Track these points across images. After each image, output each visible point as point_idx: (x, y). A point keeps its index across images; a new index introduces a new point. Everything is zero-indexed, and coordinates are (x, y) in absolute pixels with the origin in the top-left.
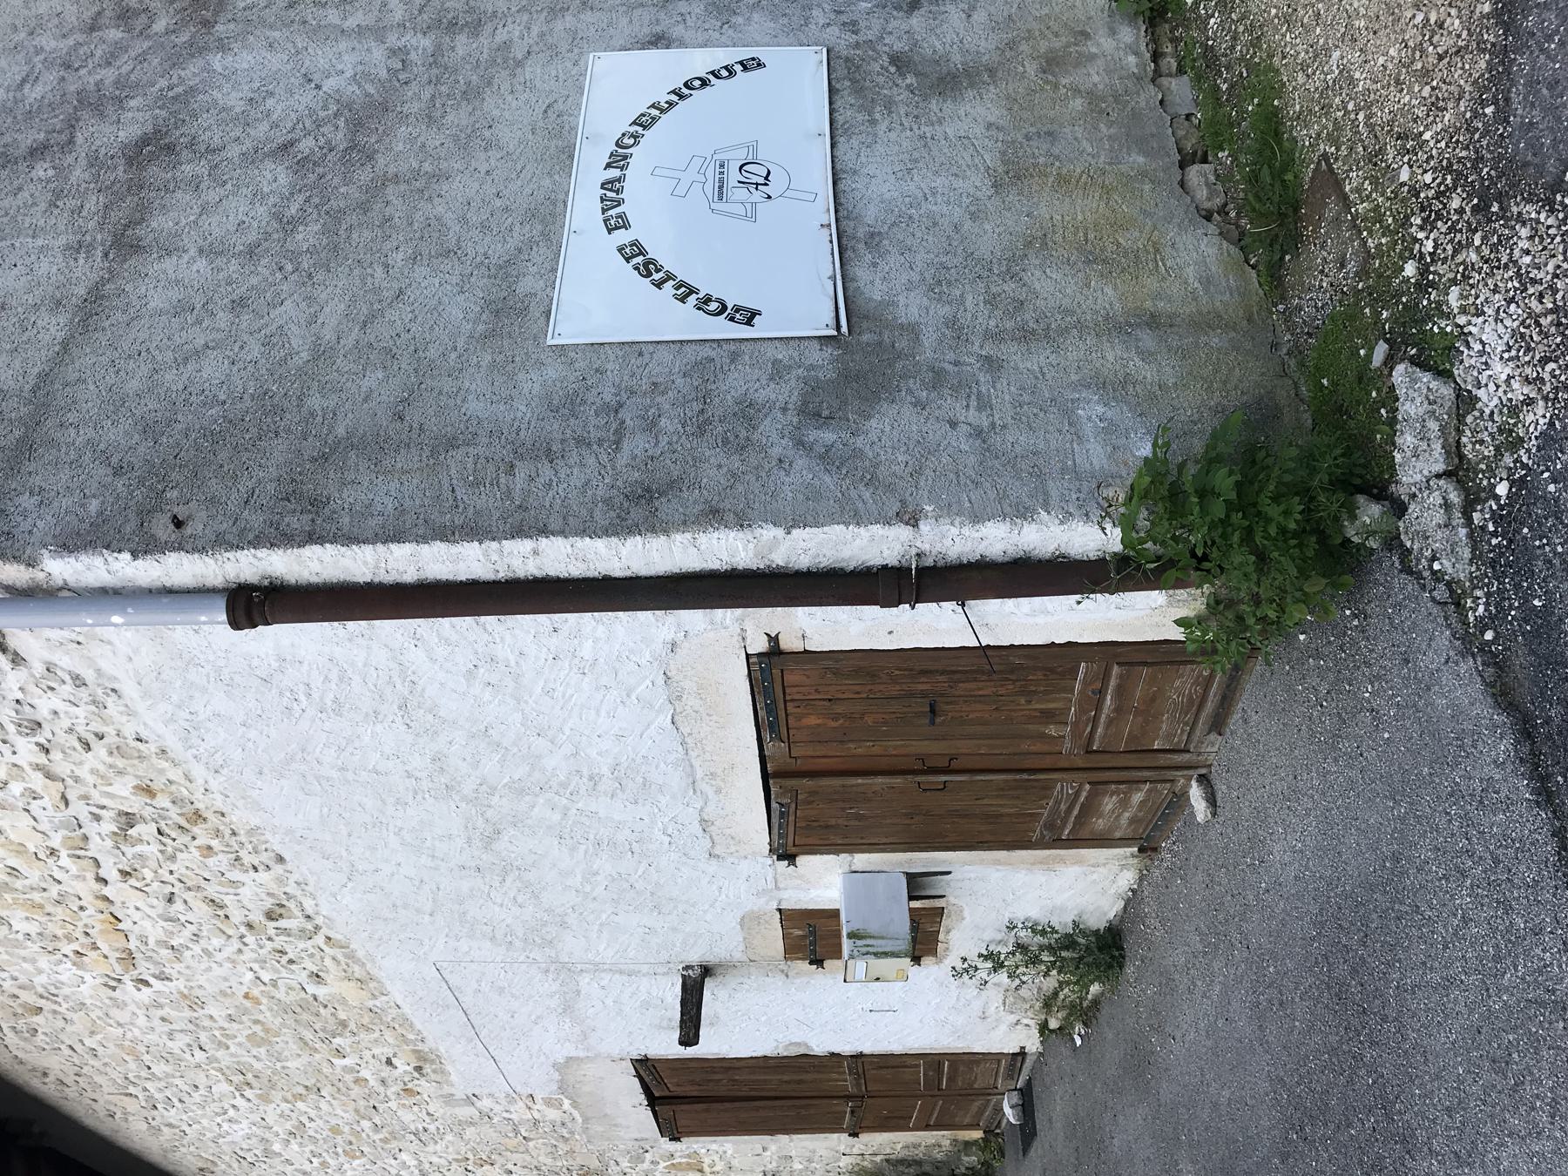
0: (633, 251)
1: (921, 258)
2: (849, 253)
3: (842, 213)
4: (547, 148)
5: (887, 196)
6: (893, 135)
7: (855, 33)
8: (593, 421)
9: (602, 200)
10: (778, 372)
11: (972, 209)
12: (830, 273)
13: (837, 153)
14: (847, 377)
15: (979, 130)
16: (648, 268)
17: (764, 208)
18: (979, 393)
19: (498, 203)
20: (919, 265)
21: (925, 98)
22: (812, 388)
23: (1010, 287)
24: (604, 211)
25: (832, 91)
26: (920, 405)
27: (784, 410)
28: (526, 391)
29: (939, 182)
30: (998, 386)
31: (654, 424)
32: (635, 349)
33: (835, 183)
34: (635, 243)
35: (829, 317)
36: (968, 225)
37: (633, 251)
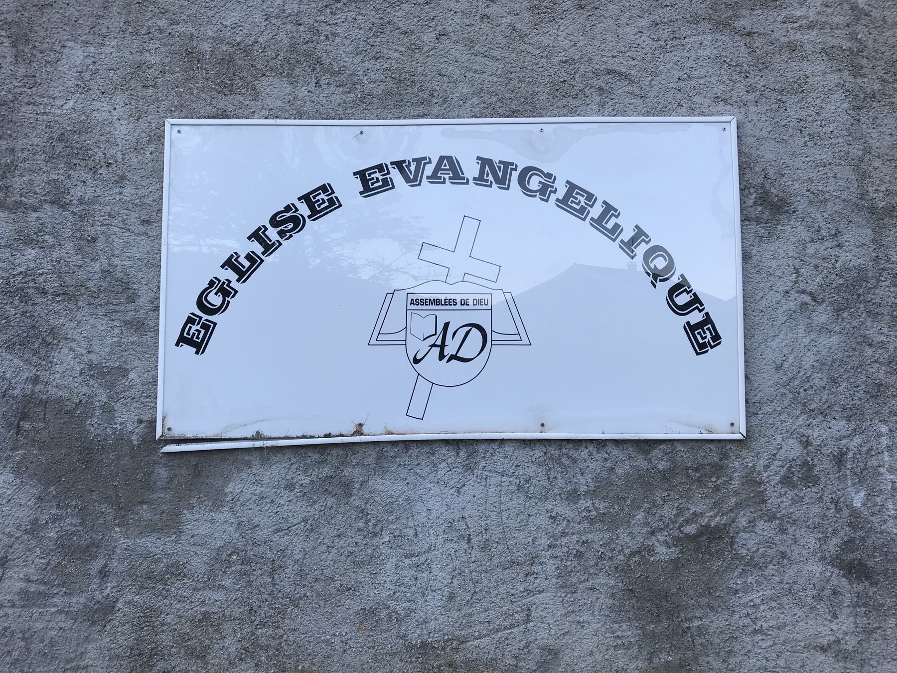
0: (320, 202)
1: (298, 545)
2: (316, 457)
3: (391, 452)
4: (533, 82)
5: (418, 507)
6: (543, 520)
7: (786, 481)
8: (38, 179)
9: (418, 161)
10: (109, 375)
11: (383, 614)
12: (266, 433)
13: (508, 448)
14: (89, 453)
15: (543, 635)
16: (288, 222)
17: (398, 357)
18: (54, 595)
19: (428, 37)
20: (280, 541)
21: (621, 570)
22: (73, 413)
23: (232, 645)
24: (399, 165)
25: (645, 446)
26: (35, 528)
27: (35, 381)
28: (97, 105)
29: (441, 576)
30: (62, 617)
31: (29, 242)
32: (151, 219)
33: (447, 442)
34: (334, 204)
35: (178, 431)
36: (352, 604)
37: (320, 202)
